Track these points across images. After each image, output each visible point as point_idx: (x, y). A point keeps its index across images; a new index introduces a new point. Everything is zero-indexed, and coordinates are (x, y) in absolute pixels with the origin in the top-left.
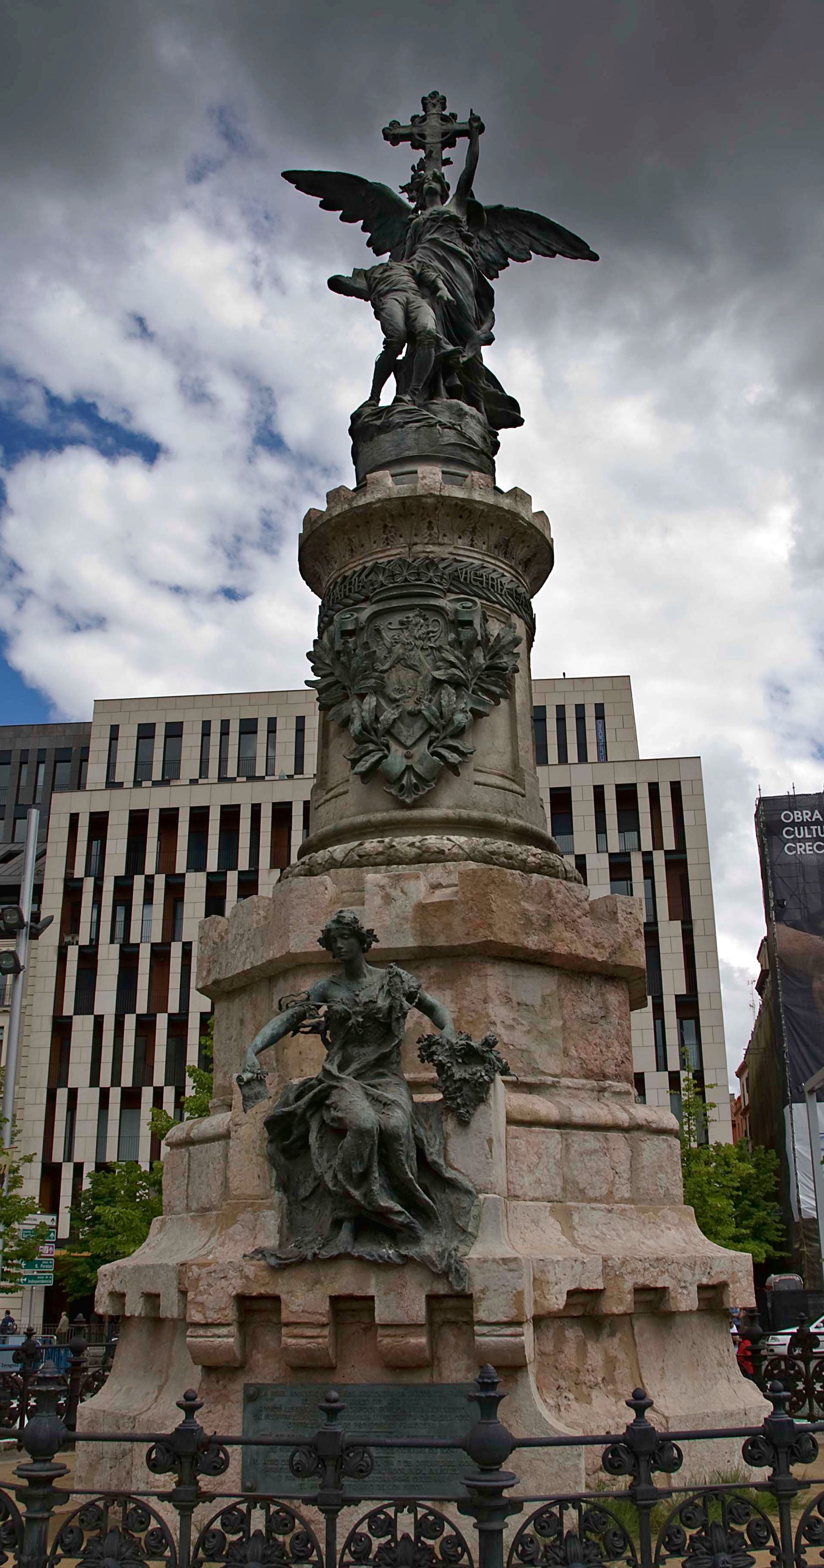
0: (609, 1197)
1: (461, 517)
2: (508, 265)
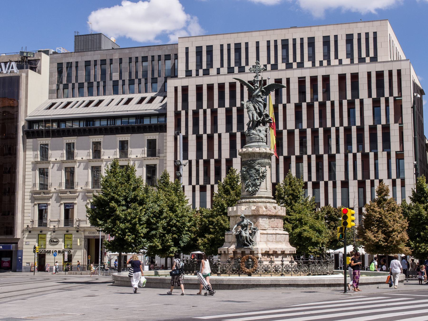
0: (273, 241)
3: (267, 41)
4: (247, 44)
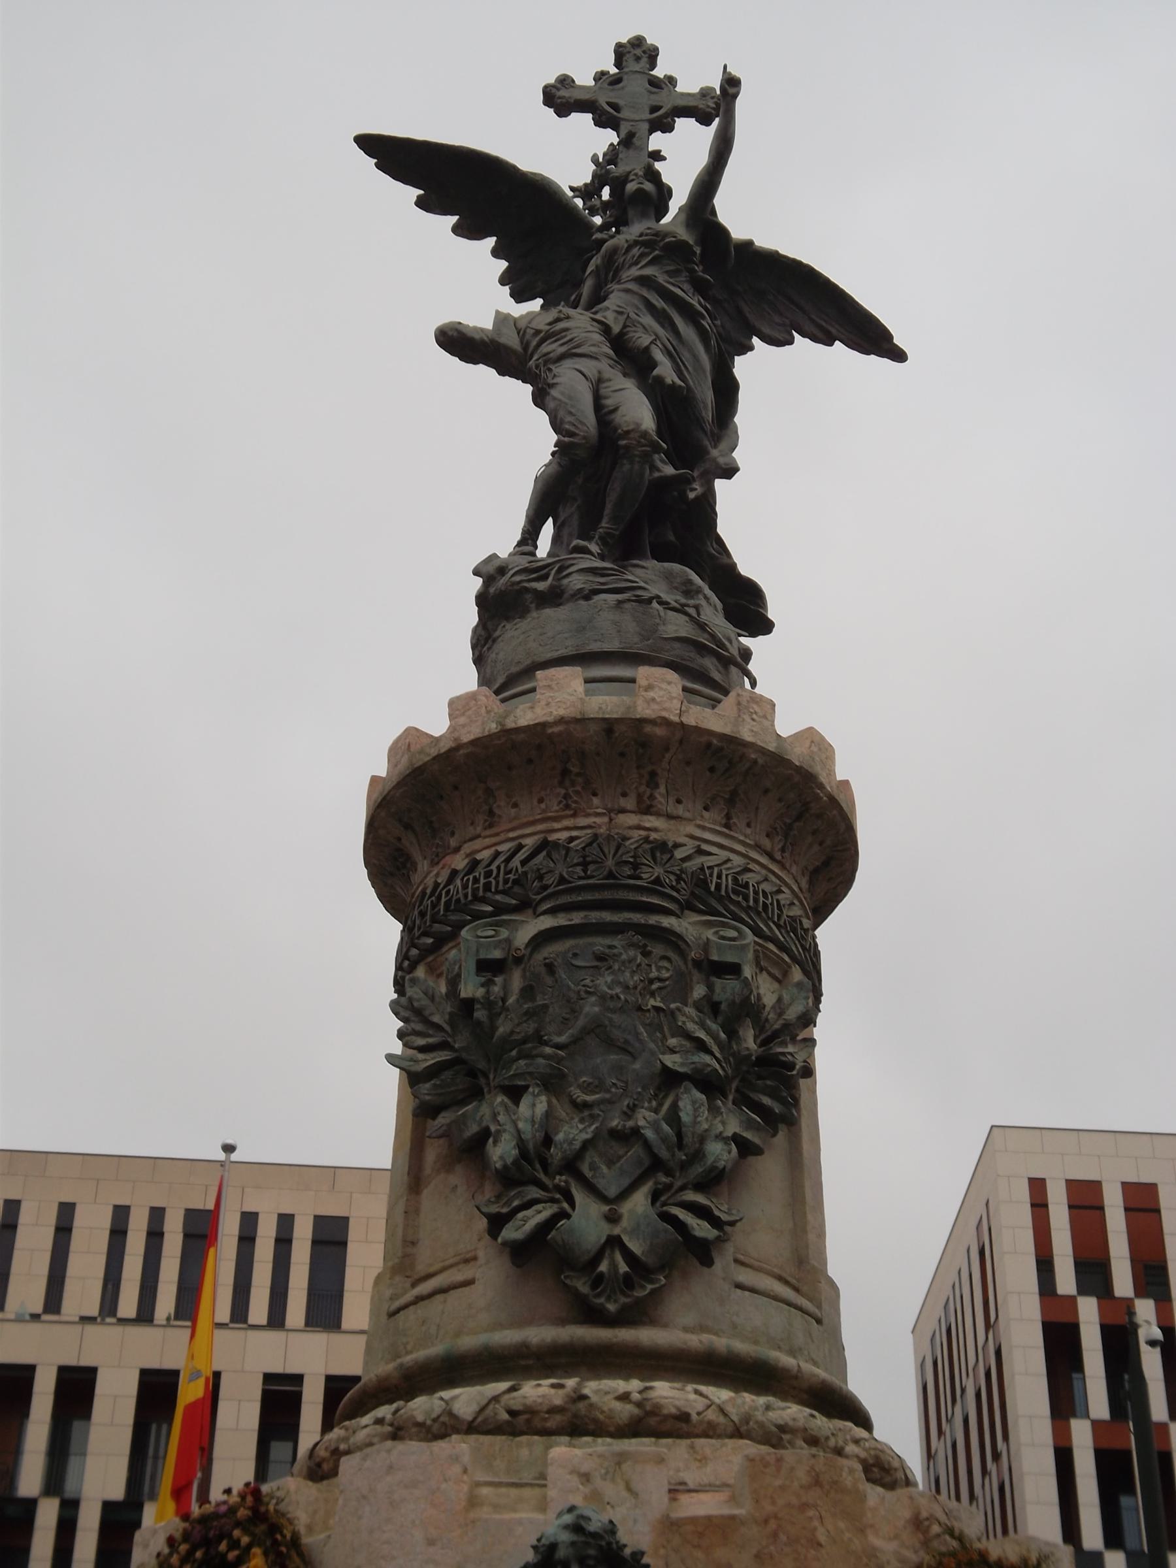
1: (712, 769)
2: (751, 348)
3: (117, 1208)
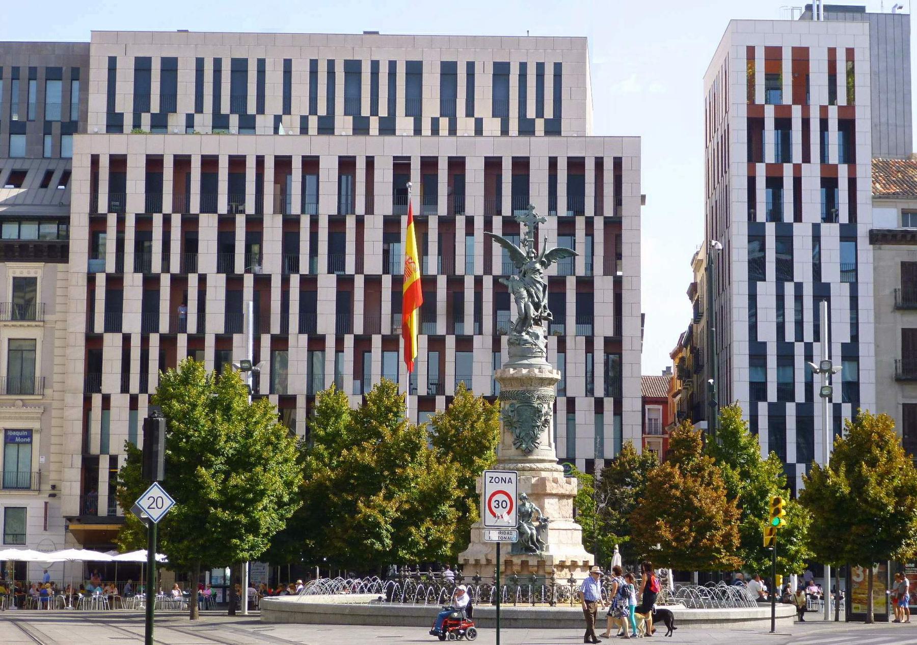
4: (261, 63)
